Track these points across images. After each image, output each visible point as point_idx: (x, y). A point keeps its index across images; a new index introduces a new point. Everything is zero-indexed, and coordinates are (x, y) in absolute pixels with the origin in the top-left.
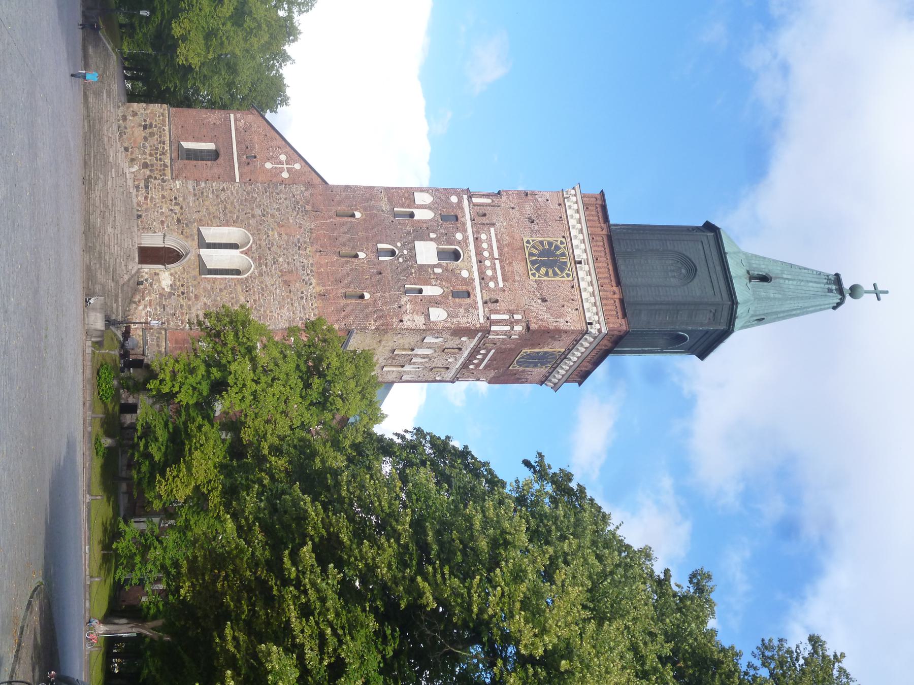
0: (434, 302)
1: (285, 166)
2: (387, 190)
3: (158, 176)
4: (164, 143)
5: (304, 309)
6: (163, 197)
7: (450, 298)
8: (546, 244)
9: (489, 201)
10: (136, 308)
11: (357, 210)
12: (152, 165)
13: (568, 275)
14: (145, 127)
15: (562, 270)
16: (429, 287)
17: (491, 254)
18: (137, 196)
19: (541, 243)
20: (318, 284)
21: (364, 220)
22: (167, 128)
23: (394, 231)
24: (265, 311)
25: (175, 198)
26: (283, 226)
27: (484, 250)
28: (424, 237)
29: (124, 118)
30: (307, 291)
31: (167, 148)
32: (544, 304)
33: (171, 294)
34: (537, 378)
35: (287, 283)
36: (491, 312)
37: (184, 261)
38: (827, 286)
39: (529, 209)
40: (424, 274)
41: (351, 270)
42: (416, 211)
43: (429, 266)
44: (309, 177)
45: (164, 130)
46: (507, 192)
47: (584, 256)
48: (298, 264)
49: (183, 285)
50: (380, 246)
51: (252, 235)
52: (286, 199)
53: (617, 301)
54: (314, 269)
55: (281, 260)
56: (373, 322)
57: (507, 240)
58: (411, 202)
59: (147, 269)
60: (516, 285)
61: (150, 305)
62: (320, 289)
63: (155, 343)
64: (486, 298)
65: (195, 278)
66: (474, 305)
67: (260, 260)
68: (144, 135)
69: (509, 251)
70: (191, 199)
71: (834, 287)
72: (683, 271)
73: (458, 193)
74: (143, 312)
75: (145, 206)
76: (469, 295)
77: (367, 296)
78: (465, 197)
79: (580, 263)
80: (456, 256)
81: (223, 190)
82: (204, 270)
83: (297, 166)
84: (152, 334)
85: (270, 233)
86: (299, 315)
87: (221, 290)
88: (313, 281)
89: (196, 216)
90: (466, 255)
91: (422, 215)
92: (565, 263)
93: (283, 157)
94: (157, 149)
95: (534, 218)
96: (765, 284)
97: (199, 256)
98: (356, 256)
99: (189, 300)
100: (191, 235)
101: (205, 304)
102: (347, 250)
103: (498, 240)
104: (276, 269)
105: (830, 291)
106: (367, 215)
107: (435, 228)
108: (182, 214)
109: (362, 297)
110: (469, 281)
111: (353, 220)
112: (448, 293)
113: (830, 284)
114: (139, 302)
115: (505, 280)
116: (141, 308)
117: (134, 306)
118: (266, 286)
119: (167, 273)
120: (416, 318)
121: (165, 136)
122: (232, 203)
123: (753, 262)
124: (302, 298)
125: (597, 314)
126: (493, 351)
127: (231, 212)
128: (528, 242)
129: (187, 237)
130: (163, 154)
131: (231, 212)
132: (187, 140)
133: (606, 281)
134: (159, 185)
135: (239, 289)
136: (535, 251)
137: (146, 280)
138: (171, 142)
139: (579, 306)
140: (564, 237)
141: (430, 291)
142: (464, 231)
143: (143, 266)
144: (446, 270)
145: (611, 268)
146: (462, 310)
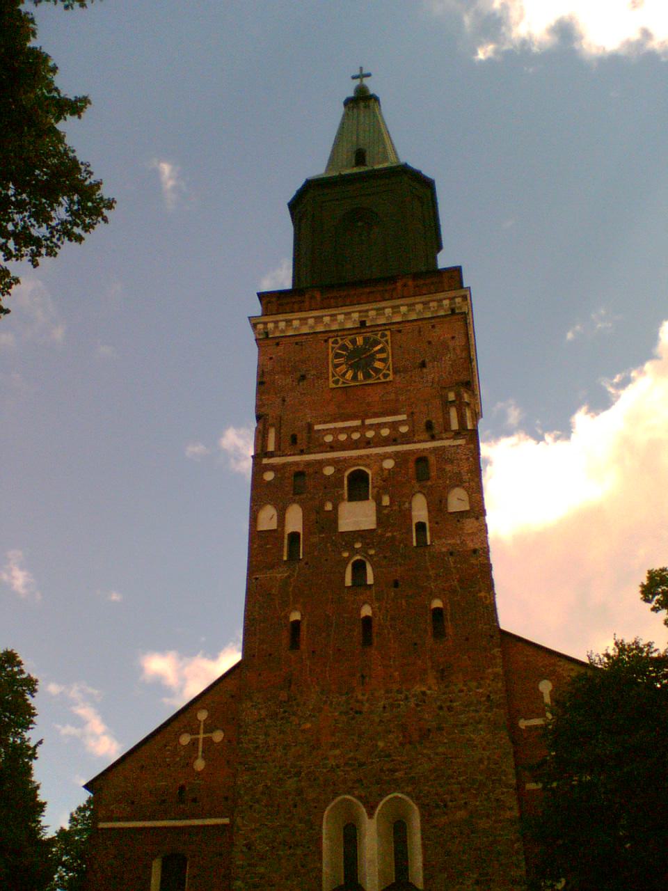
0: (438, 506)
1: (201, 736)
7: (429, 483)
8: (336, 361)
11: (287, 617)
13: (383, 336)
15: (376, 343)
16: (414, 513)
17: (356, 429)
26: (318, 740)
28: (333, 517)
35: (425, 734)
36: (447, 426)
46: (258, 407)
47: (355, 316)
50: (348, 581)
51: (336, 794)
52: (267, 734)
54: (395, 687)
55: (381, 744)
56: (482, 594)
60: (402, 398)
62: (432, 681)
64: (426, 436)
69: (350, 403)
76: (422, 460)
77: (437, 603)
78: (265, 461)
79: (363, 323)
83: (202, 715)
88: (418, 688)
90: (360, 462)
91: (295, 520)
93: (185, 739)
95: (298, 374)
98: (367, 621)
102: (357, 632)
103: (335, 420)
110: (400, 458)
124: (450, 709)
128: (336, 382)
136: (350, 375)
140: (326, 341)
141: (420, 510)
142: (322, 464)
146: (448, 468)
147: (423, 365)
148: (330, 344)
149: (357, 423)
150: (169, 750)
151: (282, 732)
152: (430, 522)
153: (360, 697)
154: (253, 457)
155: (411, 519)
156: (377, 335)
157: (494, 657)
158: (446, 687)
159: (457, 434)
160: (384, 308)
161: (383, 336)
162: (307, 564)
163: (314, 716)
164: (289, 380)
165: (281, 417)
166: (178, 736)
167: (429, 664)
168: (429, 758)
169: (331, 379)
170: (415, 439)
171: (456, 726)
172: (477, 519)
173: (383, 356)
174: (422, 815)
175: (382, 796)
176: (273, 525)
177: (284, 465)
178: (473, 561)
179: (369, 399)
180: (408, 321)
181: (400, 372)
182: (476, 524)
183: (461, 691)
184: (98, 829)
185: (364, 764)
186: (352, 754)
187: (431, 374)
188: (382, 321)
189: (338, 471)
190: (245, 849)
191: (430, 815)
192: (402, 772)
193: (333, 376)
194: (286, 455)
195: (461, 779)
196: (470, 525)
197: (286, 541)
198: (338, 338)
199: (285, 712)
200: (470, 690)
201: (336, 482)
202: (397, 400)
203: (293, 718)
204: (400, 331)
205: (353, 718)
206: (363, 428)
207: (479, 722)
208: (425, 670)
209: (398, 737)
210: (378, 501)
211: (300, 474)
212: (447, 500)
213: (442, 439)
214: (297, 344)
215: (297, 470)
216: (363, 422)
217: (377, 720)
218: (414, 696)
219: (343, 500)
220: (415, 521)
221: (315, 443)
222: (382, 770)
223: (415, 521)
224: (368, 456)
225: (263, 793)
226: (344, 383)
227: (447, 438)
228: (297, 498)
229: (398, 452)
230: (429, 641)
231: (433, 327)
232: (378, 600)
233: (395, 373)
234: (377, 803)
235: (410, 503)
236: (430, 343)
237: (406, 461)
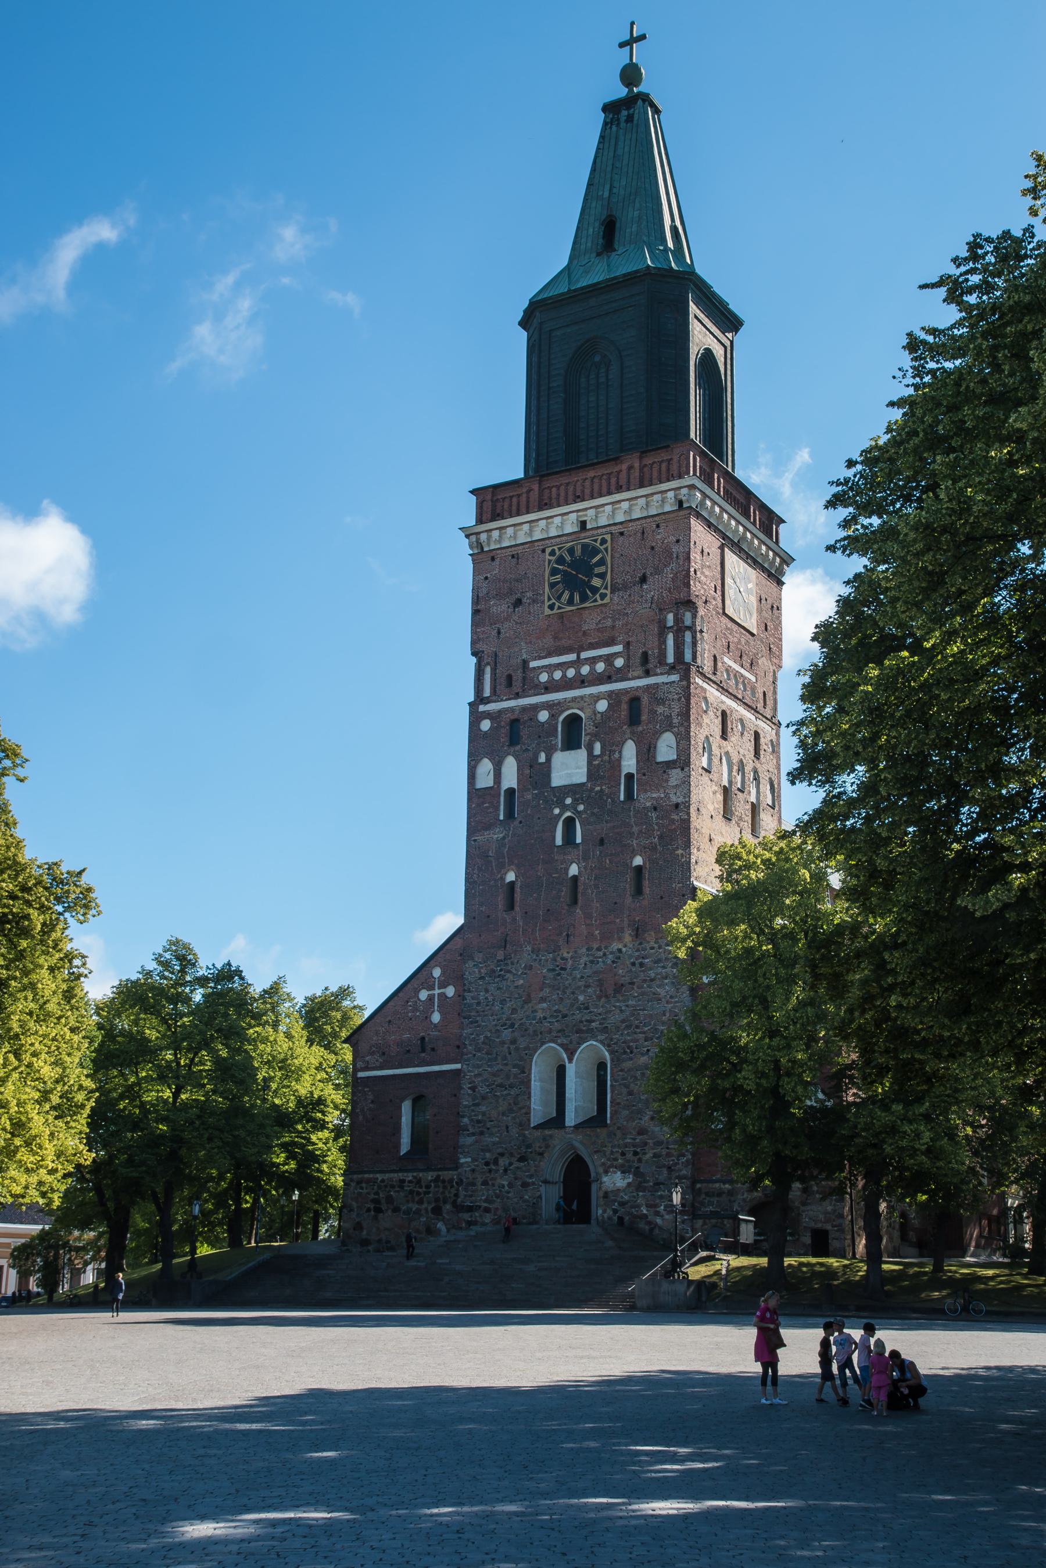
1: (437, 992)
2: (471, 831)
3: (453, 1191)
4: (403, 1181)
5: (658, 961)
6: (485, 1183)
7: (640, 728)
8: (553, 579)
9: (488, 670)
10: (660, 1228)
11: (503, 879)
12: (437, 1200)
13: (604, 541)
14: (378, 1210)
15: (595, 551)
16: (624, 763)
18: (484, 1224)
19: (552, 586)
20: (620, 939)
22: (380, 1177)
24: (663, 1023)
25: (487, 1164)
26: (529, 995)
27: (564, 675)
28: (546, 770)
29: (365, 1243)
30: (630, 959)
31: (409, 1176)
32: (650, 580)
33: (637, 1173)
34: (772, 586)
35: (619, 988)
37: (584, 1154)
38: (623, 125)
39: (500, 608)
40: (603, 770)
41: (596, 886)
43: (590, 763)
44: (451, 954)
45: (383, 1181)
46: (473, 643)
48: (588, 971)
49: (623, 1154)
50: (559, 841)
52: (487, 991)
54: (595, 946)
55: (581, 998)
56: (680, 852)
57: (548, 641)
58: (492, 792)
59: (598, 1211)
60: (619, 624)
61: (656, 1206)
62: (627, 939)
63: (715, 1200)
64: (639, 671)
65: (611, 1135)
67: (583, 1033)
68: (390, 1212)
69: (567, 637)
70: (488, 1139)
71: (624, 113)
72: (597, 358)
73: (475, 718)
74: (667, 1217)
75: (500, 1212)
76: (634, 702)
77: (638, 861)
80: (574, 721)
81: (473, 1089)
82: (596, 1121)
83: (437, 972)
84: (702, 1203)
85: (540, 1015)
86: (668, 969)
87: (631, 1093)
88: (615, 946)
89: (514, 1131)
91: (510, 777)
92: (585, 546)
93: (423, 995)
94: (411, 1192)
95: (512, 599)
96: (618, 225)
97: (577, 1127)
99: (646, 1144)
100: (544, 1139)
101: (652, 1118)
102: (565, 892)
103: (549, 655)
105: (630, 119)
106: (511, 863)
107: (531, 754)
108: (512, 1155)
109: (639, 869)
111: (518, 885)
112: (633, 733)
113: (618, 120)
114: (649, 1223)
115: (611, 642)
116: (659, 1221)
117: (657, 1231)
118: (623, 1021)
119: (605, 1179)
120: (673, 782)
121: (391, 1179)
122: (494, 1075)
123: (583, 247)
124: (641, 965)
126: (726, 659)
127: (508, 1077)
128: (551, 607)
129: (547, 1146)
130: (419, 1182)
131: (508, 1077)
132: (398, 1145)
133: (613, 480)
134: (466, 1190)
135: (628, 1064)
136: (566, 595)
137: (615, 1211)
138: (400, 1170)
140: (543, 551)
141: (629, 762)
142: (536, 708)
143: (593, 1217)
144: (596, 736)
145: (591, 474)
147: (643, 579)
149: (573, 657)
151: (499, 989)
153: (565, 955)
154: (470, 704)
155: (620, 771)
156: (596, 541)
158: (641, 944)
159: (672, 668)
160: (603, 505)
162: (521, 822)
164: (504, 607)
165: (496, 655)
166: (417, 992)
168: (621, 1011)
171: (645, 981)
172: (683, 769)
173: (602, 569)
175: (580, 1044)
176: (491, 783)
177: (500, 712)
178: (676, 817)
179: (585, 627)
180: (631, 521)
181: (619, 590)
182: (681, 775)
183: (652, 948)
184: (358, 1078)
187: (652, 590)
188: (603, 521)
189: (553, 717)
190: (470, 1092)
193: (549, 599)
194: (502, 700)
196: (675, 775)
197: (502, 799)
198: (556, 548)
200: (660, 947)
201: (548, 730)
202: (614, 627)
203: (508, 975)
205: (559, 974)
206: (578, 663)
207: (666, 978)
208: (622, 928)
209: (595, 991)
210: (590, 749)
211: (514, 723)
212: (655, 747)
213: (656, 675)
214: (513, 556)
215: (512, 718)
216: (578, 657)
218: (612, 953)
219: (556, 750)
220: (624, 771)
222: (581, 1022)
223: (624, 771)
224: (582, 697)
225: (483, 1043)
226: (559, 608)
227: (662, 674)
228: (512, 750)
229: (612, 692)
230: (629, 900)
231: (658, 526)
232: (585, 858)
234: (576, 1051)
235: (620, 752)
236: (653, 548)
237: (620, 702)
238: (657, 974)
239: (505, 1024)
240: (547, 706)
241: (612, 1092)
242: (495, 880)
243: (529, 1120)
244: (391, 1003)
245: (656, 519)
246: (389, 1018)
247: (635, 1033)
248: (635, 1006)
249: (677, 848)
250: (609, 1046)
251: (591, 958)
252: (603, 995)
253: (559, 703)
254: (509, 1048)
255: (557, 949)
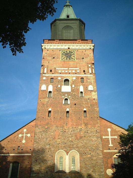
0: (86, 88)
1: (25, 135)
7: (84, 83)
8: (62, 55)
9: (46, 69)
15: (72, 52)
17: (66, 70)
20: (81, 126)
21: (52, 107)
23: (57, 98)
24: (94, 147)
26: (55, 137)
28: (60, 89)
30: (84, 130)
36: (88, 72)
42: (49, 91)
48: (72, 133)
50: (63, 103)
51: (59, 150)
52: (42, 135)
53: (82, 42)
54: (74, 127)
55: (70, 139)
56: (96, 108)
57: (61, 65)
62: (83, 126)
66: (87, 77)
77: (85, 109)
78: (44, 75)
79: (69, 48)
80: (67, 80)
83: (25, 130)
85: (58, 142)
87: (86, 164)
90: (67, 77)
101: (93, 171)
103: (61, 67)
104: (75, 142)
106: (50, 106)
107: (56, 85)
110: (77, 78)
115: (76, 67)
118: (83, 146)
124: (87, 132)
125: (87, 46)
128: (62, 60)
135: (85, 157)
139: (84, 51)
141: (81, 89)
142: (58, 77)
145: (70, 42)
147: (83, 58)
148: (61, 52)
149: (67, 69)
150: (16, 138)
151: (46, 135)
152: (84, 91)
153: (66, 128)
157: (98, 122)
161: (74, 51)
163: (54, 132)
166: (18, 135)
167: (83, 122)
168: (82, 143)
169: (61, 59)
170: (81, 74)
171: (88, 136)
173: (74, 55)
174: (80, 155)
175: (70, 151)
178: (94, 101)
183: (90, 129)
185: (66, 143)
186: (63, 141)
191: (82, 155)
192: (75, 145)
193: (61, 58)
195: (89, 148)
199: (46, 131)
203: (48, 132)
204: (78, 51)
205: (64, 133)
209: (74, 138)
213: (87, 74)
214: (53, 51)
216: (68, 69)
217: (70, 134)
218: (79, 129)
220: (80, 91)
221: (56, 72)
222: (70, 145)
228: (51, 83)
232: (71, 107)
233: (76, 59)
234: (69, 152)
238: (92, 135)
239: (47, 144)
240: (61, 77)
241: (80, 164)
242: (46, 110)
243: (54, 170)
244: (10, 137)
245: (86, 50)
246: (9, 141)
247: (86, 149)
248: (86, 142)
249: (95, 108)
250: (79, 152)
251: (73, 130)
252: (77, 139)
253: (64, 76)
254: (48, 150)
255: (63, 127)
